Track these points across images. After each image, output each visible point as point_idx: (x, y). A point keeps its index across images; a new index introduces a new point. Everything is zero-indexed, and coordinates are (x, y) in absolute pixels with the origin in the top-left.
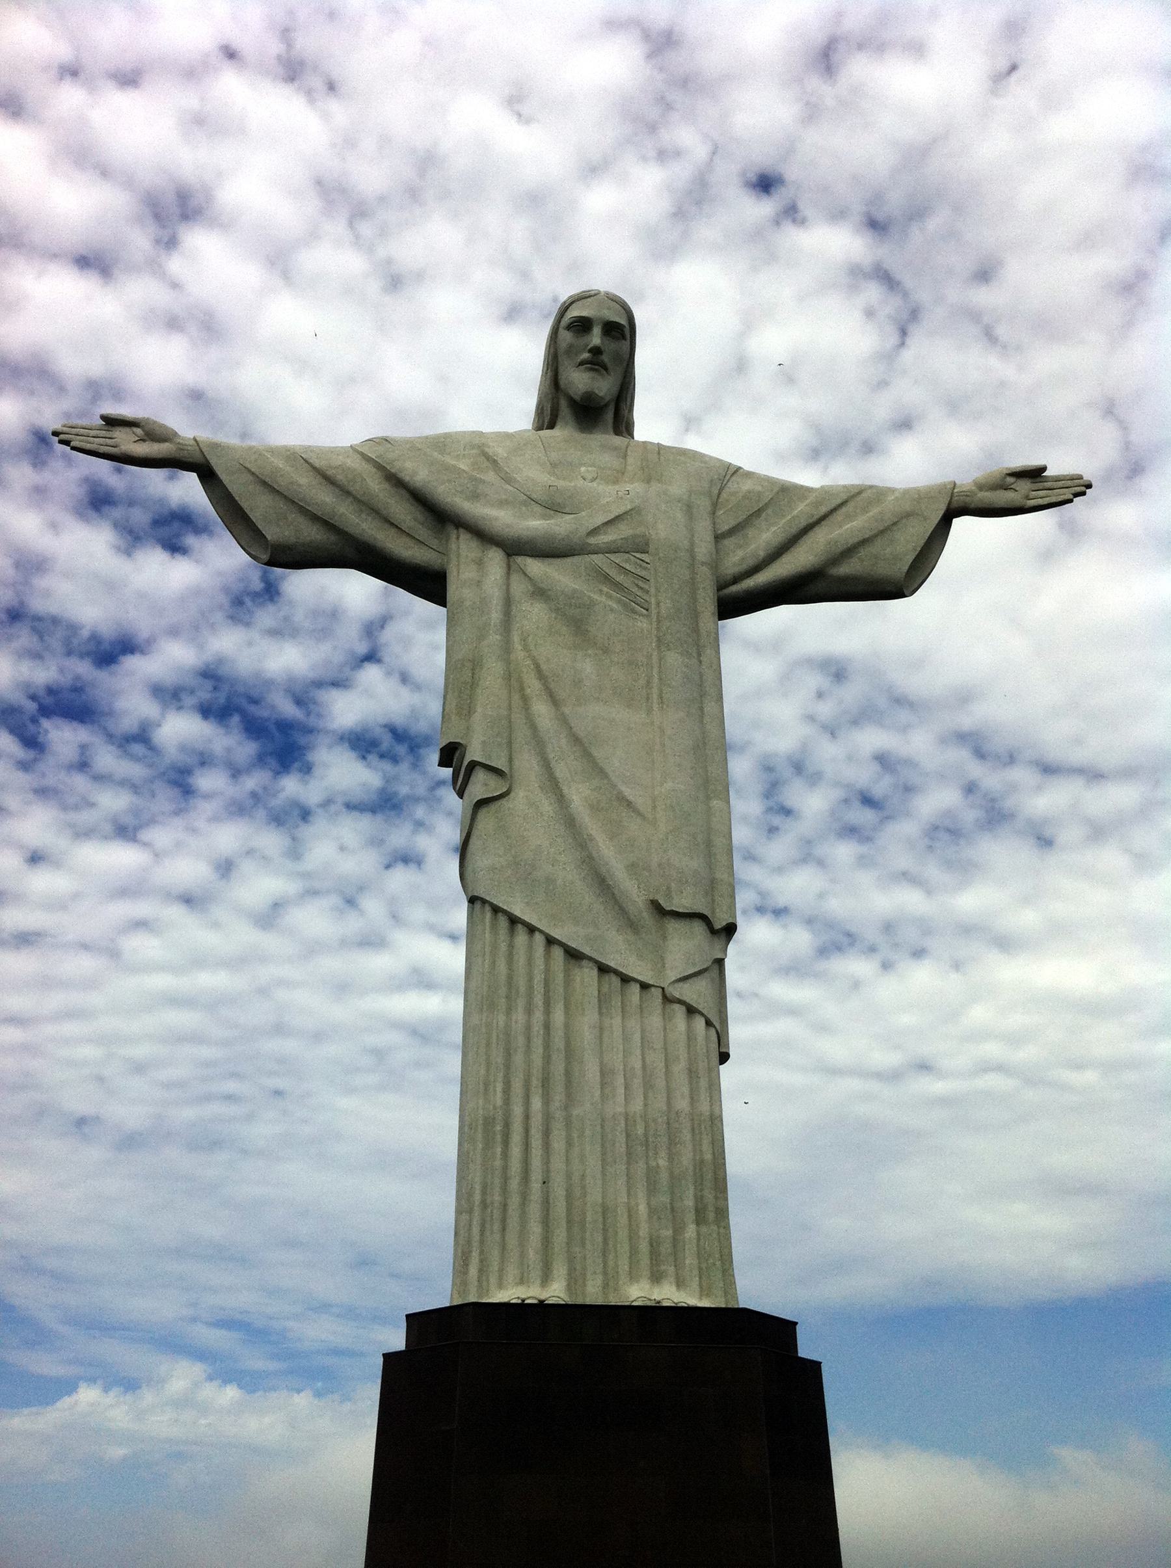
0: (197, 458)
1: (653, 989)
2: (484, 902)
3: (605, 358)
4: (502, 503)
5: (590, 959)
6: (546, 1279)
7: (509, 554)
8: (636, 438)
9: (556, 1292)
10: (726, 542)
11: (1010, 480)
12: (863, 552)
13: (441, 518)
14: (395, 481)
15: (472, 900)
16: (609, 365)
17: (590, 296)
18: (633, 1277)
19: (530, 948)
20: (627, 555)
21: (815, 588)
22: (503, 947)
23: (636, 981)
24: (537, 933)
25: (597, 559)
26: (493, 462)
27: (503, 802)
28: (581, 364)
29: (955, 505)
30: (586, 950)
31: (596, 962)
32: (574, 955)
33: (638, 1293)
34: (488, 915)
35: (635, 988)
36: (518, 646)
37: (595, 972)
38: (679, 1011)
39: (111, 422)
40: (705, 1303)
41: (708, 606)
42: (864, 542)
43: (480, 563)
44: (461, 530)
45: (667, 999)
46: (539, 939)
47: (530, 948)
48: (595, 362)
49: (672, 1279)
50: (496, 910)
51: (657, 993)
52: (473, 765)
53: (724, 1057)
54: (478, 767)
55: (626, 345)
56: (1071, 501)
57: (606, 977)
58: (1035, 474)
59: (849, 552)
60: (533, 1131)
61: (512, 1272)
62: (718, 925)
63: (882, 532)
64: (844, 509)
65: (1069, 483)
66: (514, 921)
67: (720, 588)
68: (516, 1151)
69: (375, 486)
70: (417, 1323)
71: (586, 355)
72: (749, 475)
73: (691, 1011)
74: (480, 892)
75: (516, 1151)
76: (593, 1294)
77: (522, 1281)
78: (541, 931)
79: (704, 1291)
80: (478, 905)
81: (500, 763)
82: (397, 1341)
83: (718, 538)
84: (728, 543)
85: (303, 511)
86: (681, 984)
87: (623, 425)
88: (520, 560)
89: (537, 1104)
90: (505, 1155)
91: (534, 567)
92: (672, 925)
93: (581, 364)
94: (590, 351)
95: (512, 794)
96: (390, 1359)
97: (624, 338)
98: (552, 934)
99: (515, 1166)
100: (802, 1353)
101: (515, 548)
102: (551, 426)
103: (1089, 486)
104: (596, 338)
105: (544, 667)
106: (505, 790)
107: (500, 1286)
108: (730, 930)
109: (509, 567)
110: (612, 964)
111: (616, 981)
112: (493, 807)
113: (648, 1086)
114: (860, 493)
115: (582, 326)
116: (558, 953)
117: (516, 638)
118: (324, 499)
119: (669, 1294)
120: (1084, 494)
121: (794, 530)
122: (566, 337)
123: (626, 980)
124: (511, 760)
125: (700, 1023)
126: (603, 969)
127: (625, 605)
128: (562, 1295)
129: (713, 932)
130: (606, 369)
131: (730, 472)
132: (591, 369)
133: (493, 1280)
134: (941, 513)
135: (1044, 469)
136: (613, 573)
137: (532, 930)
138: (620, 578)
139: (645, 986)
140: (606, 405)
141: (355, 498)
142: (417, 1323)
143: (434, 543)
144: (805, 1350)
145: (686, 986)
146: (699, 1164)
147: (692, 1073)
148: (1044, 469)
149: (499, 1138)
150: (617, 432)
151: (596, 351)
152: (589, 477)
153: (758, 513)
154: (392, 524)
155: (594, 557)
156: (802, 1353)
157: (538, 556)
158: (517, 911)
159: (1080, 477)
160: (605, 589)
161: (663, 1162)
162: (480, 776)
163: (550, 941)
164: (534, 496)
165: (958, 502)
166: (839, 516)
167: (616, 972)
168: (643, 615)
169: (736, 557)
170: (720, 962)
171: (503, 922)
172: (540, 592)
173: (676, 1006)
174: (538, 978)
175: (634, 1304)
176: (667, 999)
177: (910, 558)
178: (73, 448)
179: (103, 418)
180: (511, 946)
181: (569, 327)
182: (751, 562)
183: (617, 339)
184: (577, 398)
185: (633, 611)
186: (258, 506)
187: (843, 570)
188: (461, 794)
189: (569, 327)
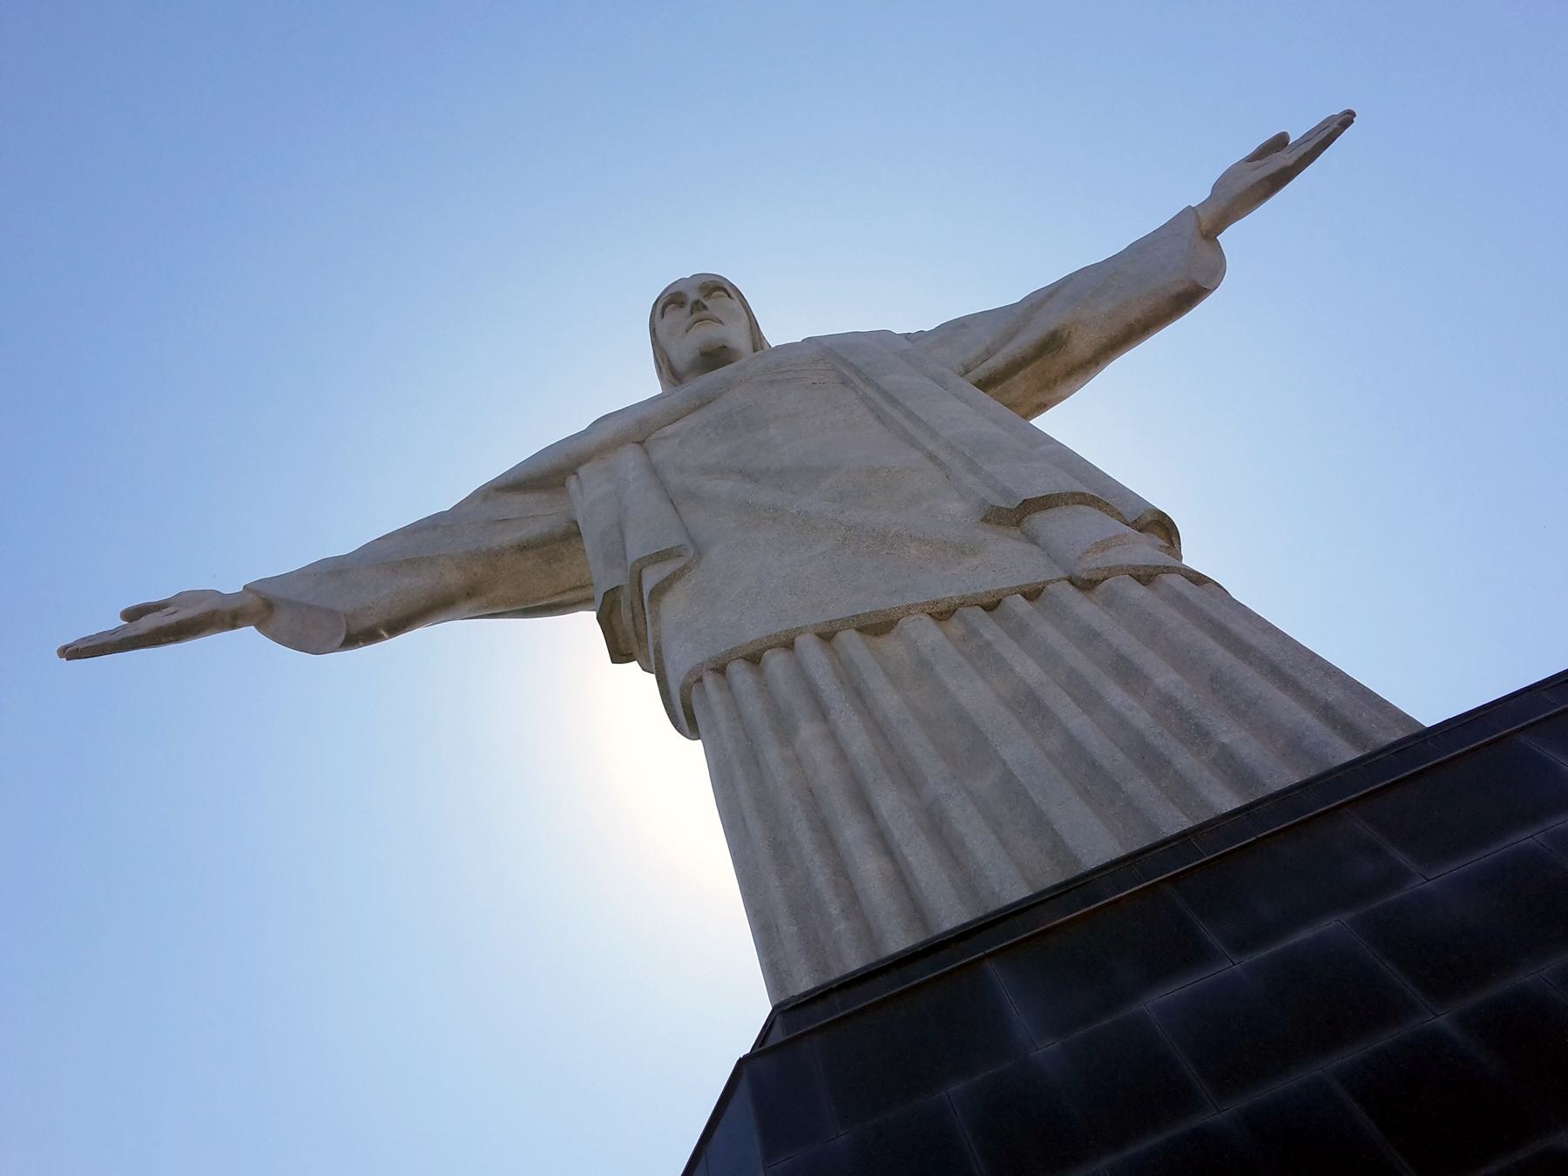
7: (641, 443)
16: (718, 315)
23: (1013, 591)
24: (799, 640)
30: (896, 602)
32: (878, 627)
39: (132, 615)
46: (808, 646)
58: (1280, 142)
62: (1130, 519)
73: (1146, 577)
78: (800, 631)
81: (674, 539)
89: (888, 801)
92: (1037, 520)
109: (647, 452)
113: (1127, 672)
116: (849, 640)
126: (942, 614)
149: (828, 895)
151: (698, 306)
158: (752, 633)
180: (765, 688)
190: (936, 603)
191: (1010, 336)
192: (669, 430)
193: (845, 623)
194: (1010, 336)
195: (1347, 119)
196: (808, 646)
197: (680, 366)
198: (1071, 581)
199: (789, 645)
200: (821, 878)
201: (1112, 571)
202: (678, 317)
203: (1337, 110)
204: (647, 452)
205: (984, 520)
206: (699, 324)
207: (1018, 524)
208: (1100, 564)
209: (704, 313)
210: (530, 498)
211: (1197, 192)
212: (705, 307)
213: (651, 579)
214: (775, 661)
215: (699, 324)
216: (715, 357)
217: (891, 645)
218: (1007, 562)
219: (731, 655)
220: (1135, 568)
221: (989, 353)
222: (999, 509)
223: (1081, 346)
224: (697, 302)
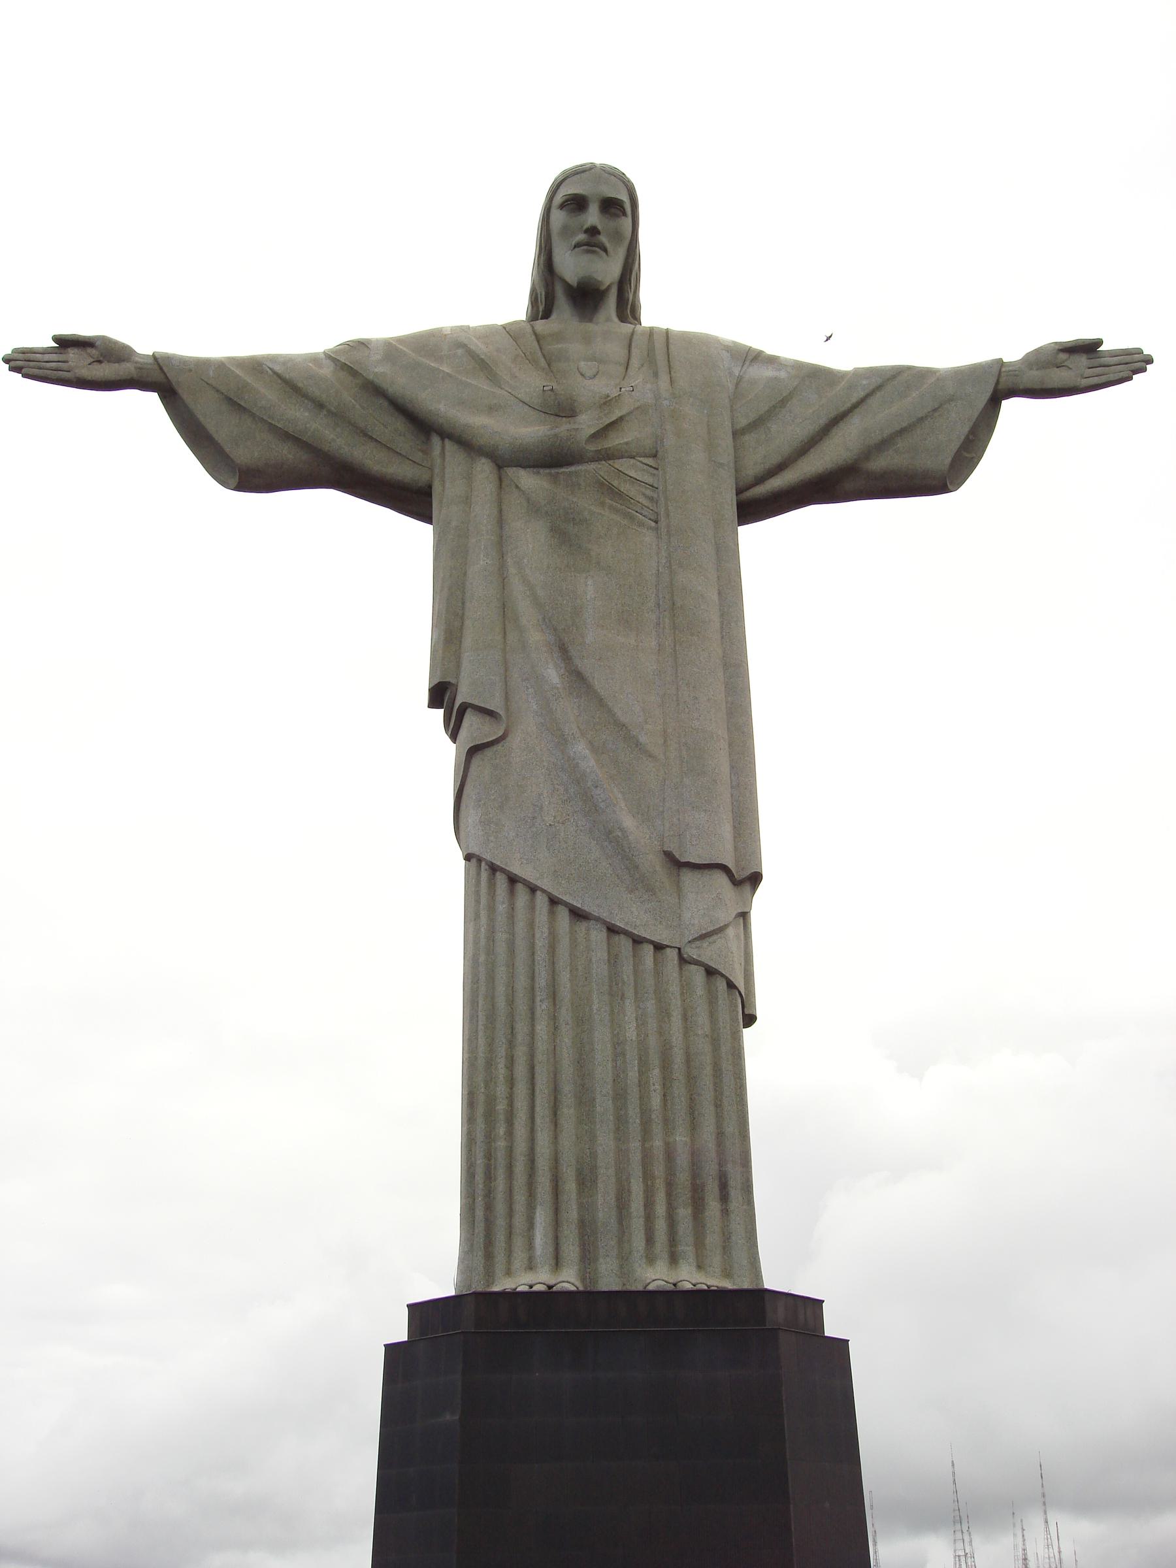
0: (157, 376)
1: (668, 950)
2: (480, 860)
3: (603, 238)
4: (491, 409)
5: (598, 919)
6: (557, 1263)
8: (643, 324)
9: (568, 1280)
10: (747, 437)
11: (1063, 356)
12: (901, 444)
13: (423, 427)
14: (374, 390)
15: (468, 858)
16: (608, 245)
17: (584, 171)
18: (651, 1260)
19: (532, 907)
20: (632, 461)
21: (849, 485)
22: (502, 908)
23: (652, 942)
24: (539, 893)
25: (601, 469)
26: (483, 365)
27: (499, 747)
28: (577, 245)
29: (1000, 387)
31: (604, 922)
32: (578, 915)
33: (656, 1276)
34: (484, 875)
35: (648, 950)
36: (512, 570)
37: (604, 933)
38: (697, 975)
39: (65, 343)
40: (728, 1285)
41: (731, 511)
42: (902, 432)
43: (469, 478)
44: (447, 441)
45: (683, 960)
46: (541, 900)
47: (532, 907)
48: (592, 242)
49: (692, 1259)
50: (494, 869)
51: (672, 954)
52: (464, 708)
53: (750, 1020)
54: (469, 711)
55: (627, 222)
56: (1130, 379)
57: (616, 938)
58: (1090, 348)
59: (883, 444)
60: (538, 1109)
61: (520, 1257)
63: (921, 420)
64: (878, 394)
65: (1128, 358)
66: (513, 880)
67: (739, 492)
68: (521, 1131)
69: (349, 397)
70: (420, 1313)
71: (581, 237)
72: (772, 360)
73: (710, 972)
74: (475, 850)
75: (521, 1131)
76: (608, 1280)
77: (531, 1267)
78: (544, 891)
79: (727, 1273)
80: (474, 861)
81: (495, 703)
82: (400, 1333)
83: (736, 434)
84: (748, 438)
85: (273, 429)
86: (698, 943)
87: (628, 309)
88: (511, 472)
90: (510, 1133)
91: (527, 480)
94: (586, 231)
95: (508, 739)
96: (393, 1352)
97: (625, 214)
98: (556, 893)
99: (521, 1147)
100: (829, 1331)
101: (504, 461)
102: (547, 315)
103: (1150, 361)
104: (593, 216)
105: (541, 593)
106: (500, 733)
107: (509, 1273)
108: (755, 879)
109: (500, 479)
111: (625, 944)
112: (489, 752)
114: (894, 377)
115: (577, 204)
116: (563, 914)
117: (509, 561)
118: (298, 416)
119: (689, 1277)
120: (1144, 370)
121: (823, 421)
122: (558, 217)
123: (637, 941)
125: (722, 985)
126: (612, 930)
127: (632, 518)
128: (572, 1280)
129: (736, 883)
130: (605, 250)
131: (750, 358)
132: (588, 252)
133: (499, 1268)
134: (988, 395)
135: (1099, 343)
136: (615, 483)
137: (533, 889)
138: (625, 487)
139: (659, 947)
140: (609, 287)
141: (329, 411)
142: (420, 1313)
143: (418, 456)
144: (831, 1330)
145: (705, 944)
146: (720, 1135)
147: (715, 1042)
148: (1099, 343)
150: (622, 318)
151: (593, 231)
152: (589, 373)
153: (783, 402)
154: (371, 438)
155: (592, 466)
156: (829, 1331)
157: (530, 467)
158: (516, 869)
159: (1139, 351)
160: (608, 501)
161: (681, 1138)
162: (470, 719)
163: (554, 901)
164: (527, 400)
165: (1005, 383)
166: (874, 401)
168: (651, 528)
169: (758, 457)
170: (744, 916)
171: (501, 881)
172: (534, 509)
173: (693, 967)
174: (541, 943)
175: (651, 1287)
176: (683, 960)
177: (955, 446)
178: (25, 376)
179: (56, 339)
181: (562, 206)
182: (776, 459)
183: (617, 216)
184: (575, 284)
185: (641, 524)
186: (223, 427)
187: (879, 463)
188: (454, 737)
189: (562, 206)
193: (566, 904)
200: (501, 1107)
206: (590, 226)
210: (400, 424)
212: (599, 233)
215: (590, 233)
216: (586, 297)
217: (582, 926)
219: (503, 870)
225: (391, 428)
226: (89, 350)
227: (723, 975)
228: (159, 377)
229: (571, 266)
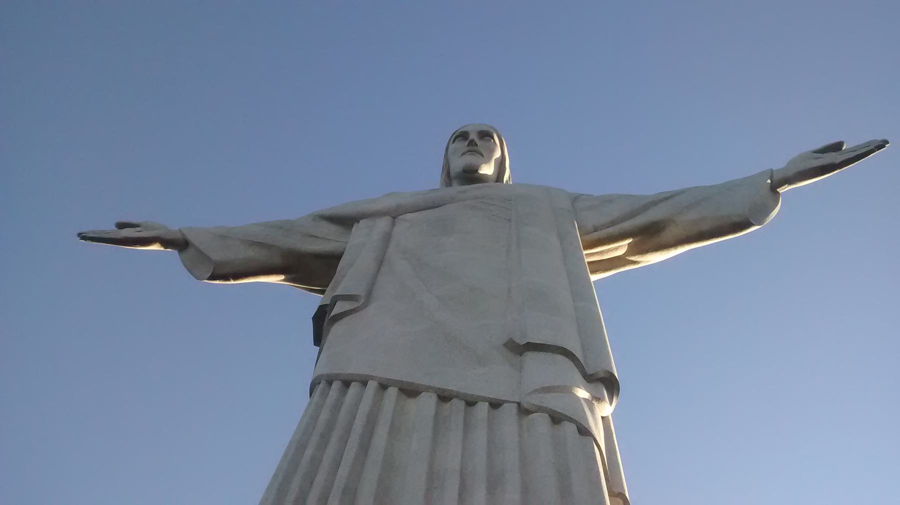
5: (428, 389)
7: (394, 218)
23: (484, 399)
32: (410, 391)
35: (482, 409)
38: (541, 421)
39: (121, 226)
45: (524, 411)
51: (509, 411)
62: (590, 371)
73: (556, 419)
78: (372, 378)
81: (359, 290)
92: (531, 358)
93: (463, 154)
110: (454, 388)
111: (458, 405)
112: (346, 320)
116: (392, 392)
124: (369, 294)
125: (569, 429)
139: (495, 405)
167: (458, 396)
176: (524, 411)
190: (444, 390)
191: (632, 215)
192: (409, 216)
194: (632, 215)
195: (881, 145)
196: (372, 385)
197: (452, 174)
198: (519, 404)
199: (364, 383)
201: (540, 409)
202: (462, 145)
203: (880, 138)
204: (393, 224)
205: (505, 345)
207: (521, 354)
208: (533, 402)
209: (475, 148)
211: (779, 163)
212: (476, 145)
213: (336, 310)
214: (354, 388)
217: (412, 405)
218: (493, 379)
220: (554, 412)
221: (613, 223)
222: (514, 342)
223: (669, 234)
224: (473, 141)
225: (328, 229)
226: (139, 229)
227: (571, 420)
228: (179, 236)
229: (458, 164)
